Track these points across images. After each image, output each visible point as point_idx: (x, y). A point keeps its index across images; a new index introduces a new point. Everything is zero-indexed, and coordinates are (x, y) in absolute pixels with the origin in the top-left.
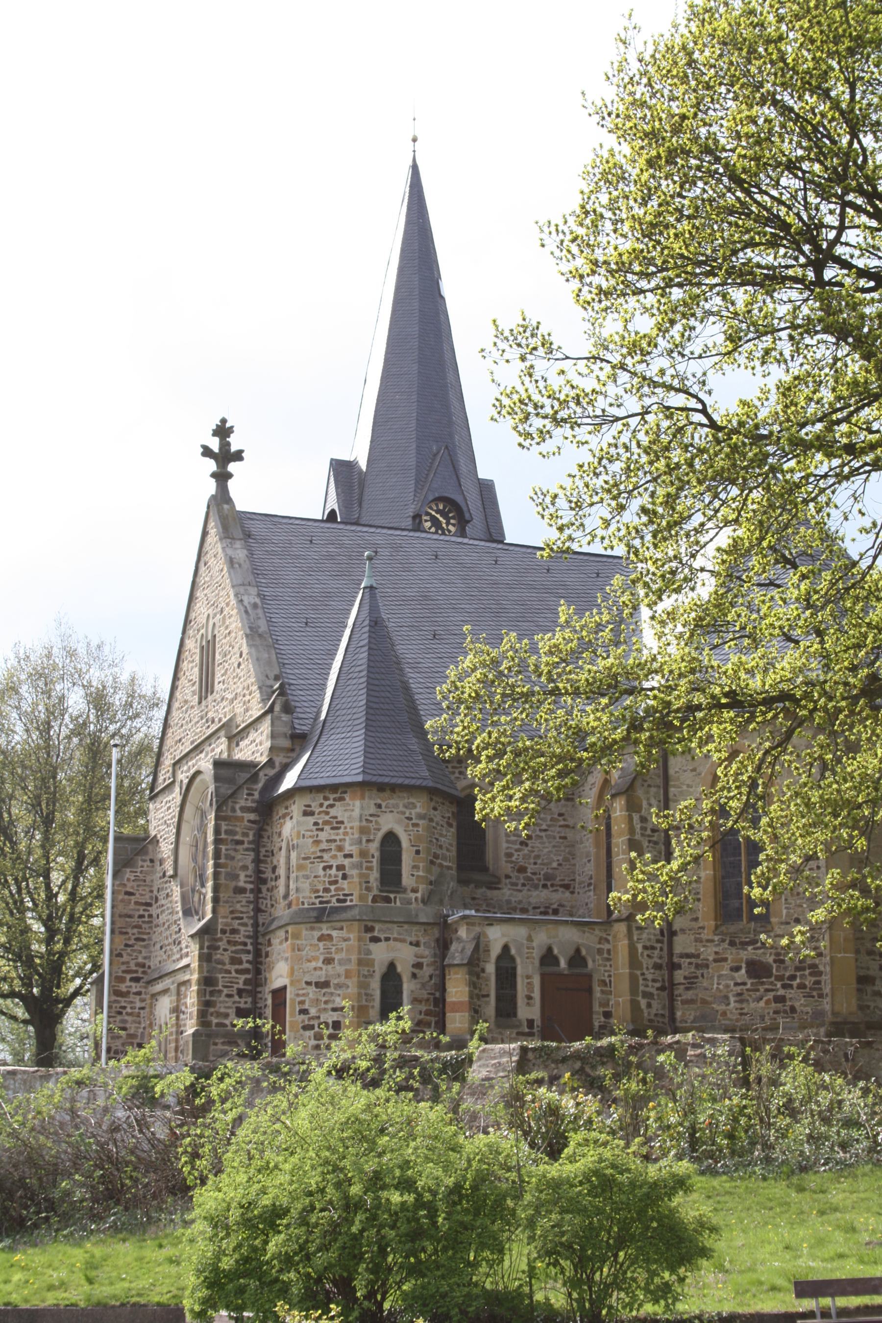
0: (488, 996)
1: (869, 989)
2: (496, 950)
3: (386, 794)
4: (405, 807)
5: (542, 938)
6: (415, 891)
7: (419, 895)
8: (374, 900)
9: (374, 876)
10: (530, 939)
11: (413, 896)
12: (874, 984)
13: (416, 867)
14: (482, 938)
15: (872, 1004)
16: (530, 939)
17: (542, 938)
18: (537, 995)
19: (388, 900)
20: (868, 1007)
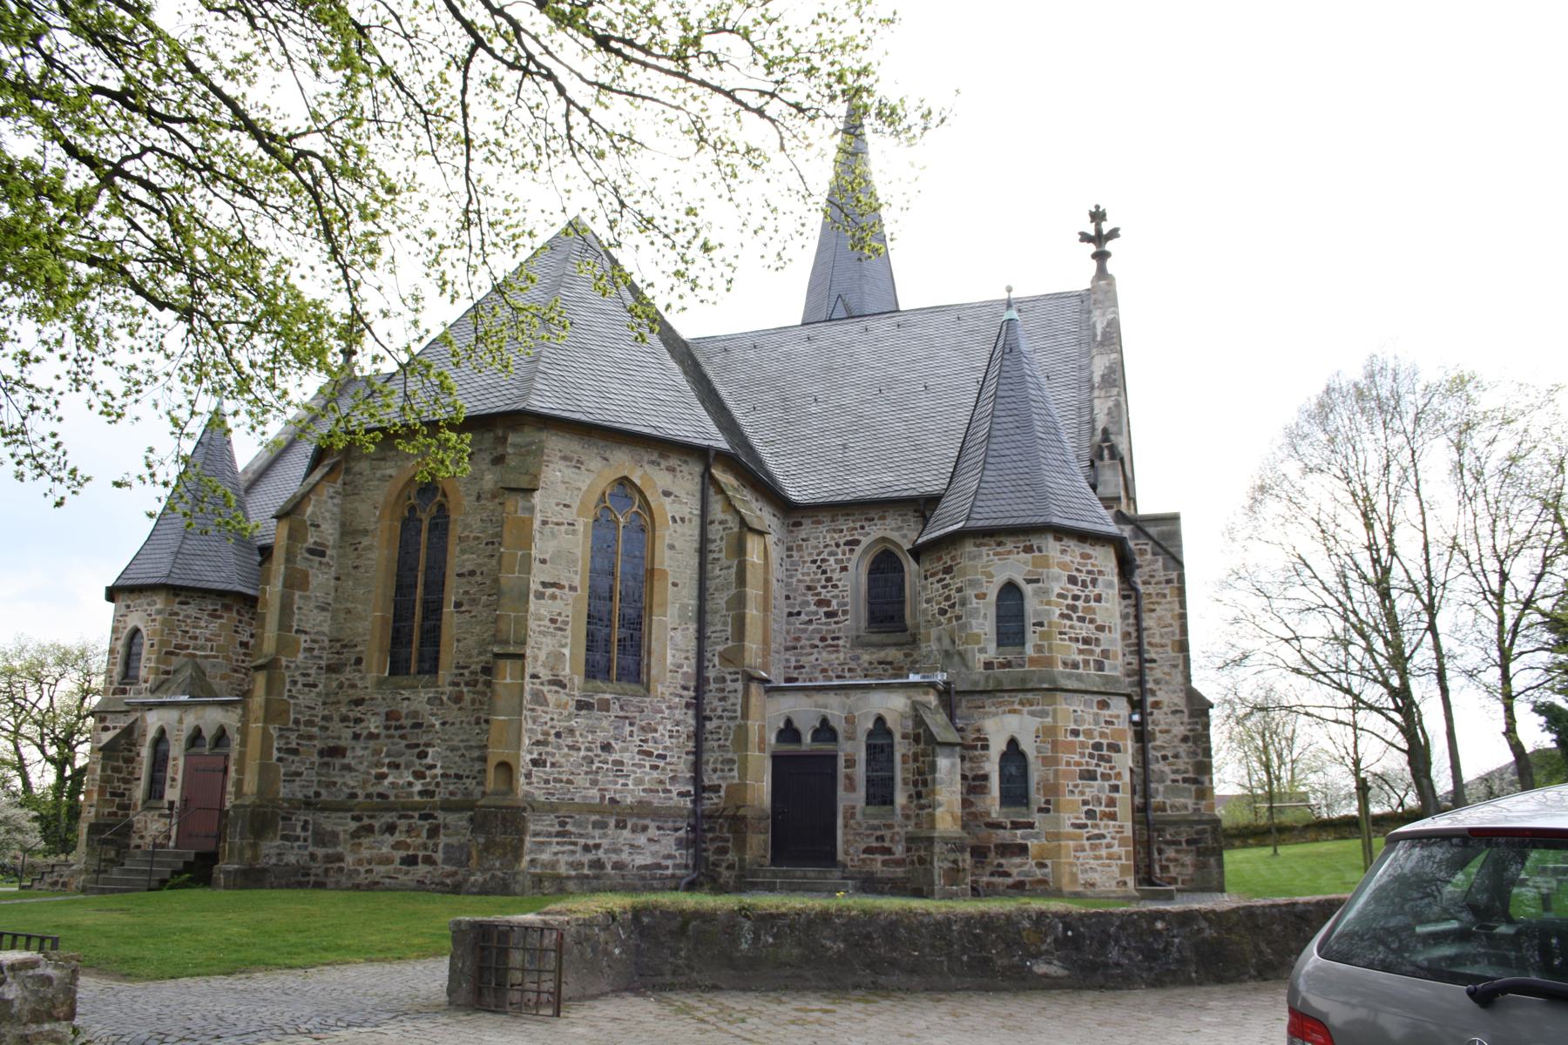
0: (139, 779)
1: (338, 762)
2: (151, 733)
3: (135, 595)
4: (149, 604)
5: (191, 720)
6: (146, 682)
7: (148, 685)
8: (114, 694)
9: (118, 670)
10: (180, 721)
11: (144, 686)
12: (344, 756)
13: (149, 659)
14: (139, 722)
15: (340, 781)
16: (180, 721)
17: (191, 720)
18: (179, 777)
19: (124, 692)
20: (335, 784)
